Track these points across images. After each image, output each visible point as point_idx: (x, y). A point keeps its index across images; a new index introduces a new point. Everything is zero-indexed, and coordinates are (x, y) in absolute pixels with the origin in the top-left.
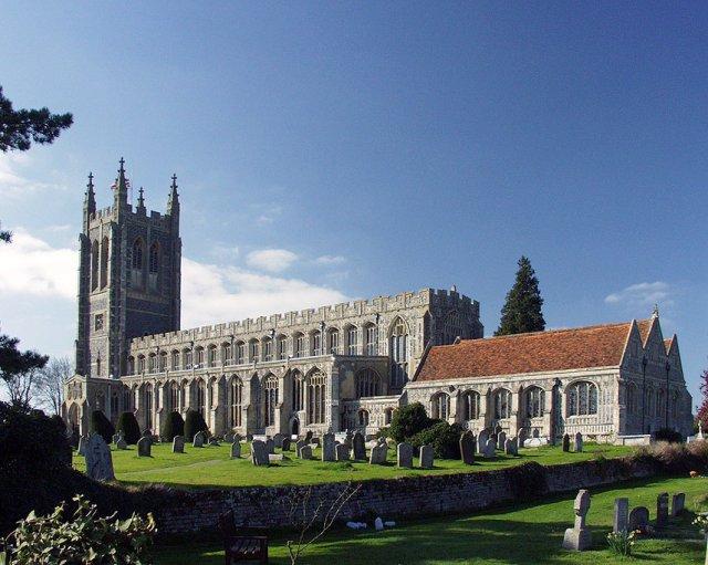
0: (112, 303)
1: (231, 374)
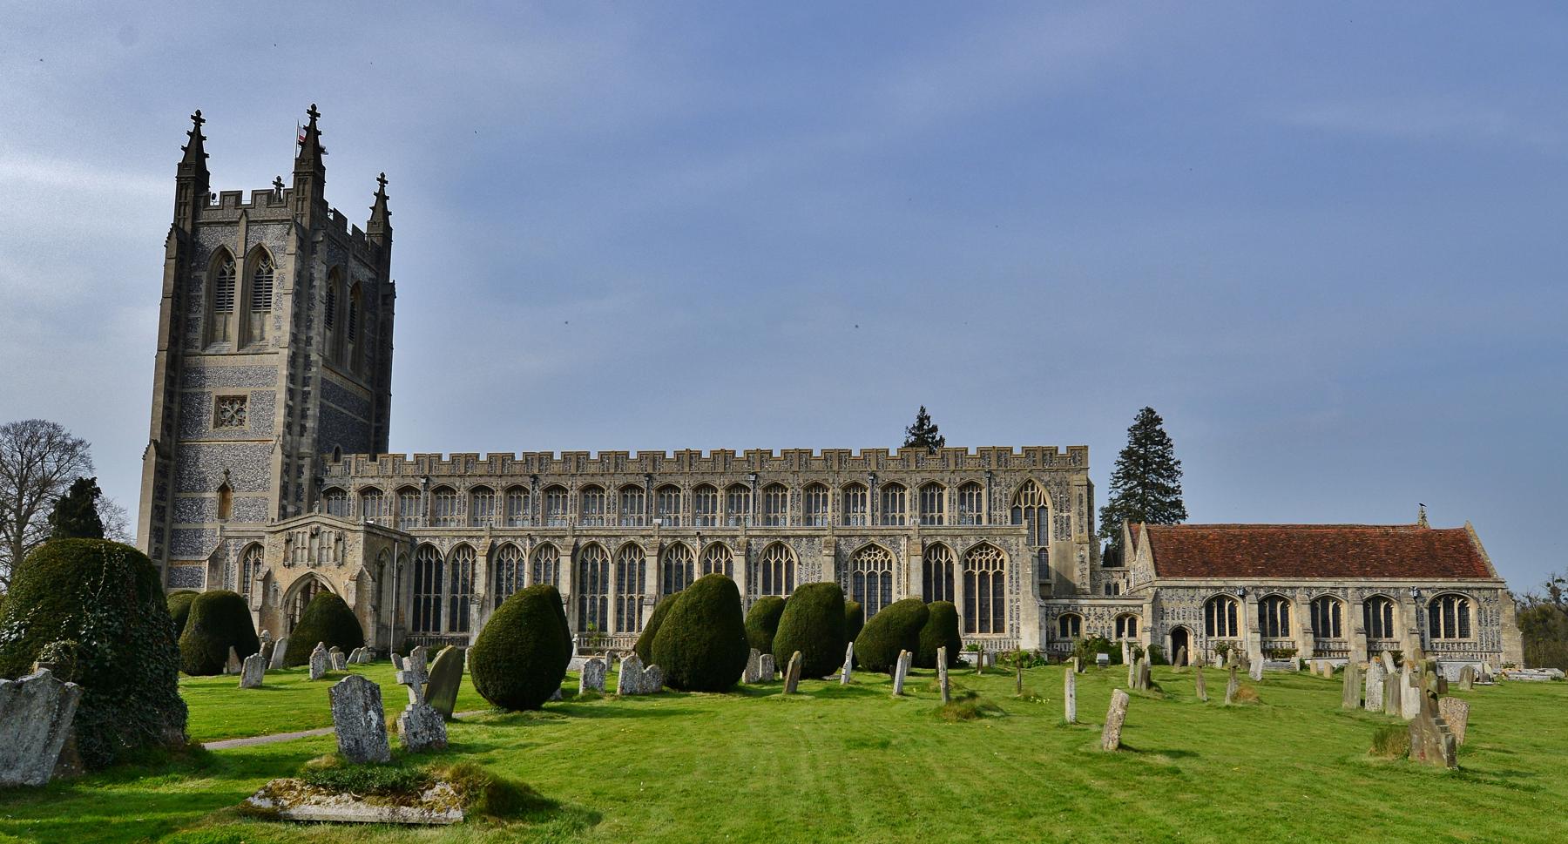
0: (292, 378)
1: (766, 542)
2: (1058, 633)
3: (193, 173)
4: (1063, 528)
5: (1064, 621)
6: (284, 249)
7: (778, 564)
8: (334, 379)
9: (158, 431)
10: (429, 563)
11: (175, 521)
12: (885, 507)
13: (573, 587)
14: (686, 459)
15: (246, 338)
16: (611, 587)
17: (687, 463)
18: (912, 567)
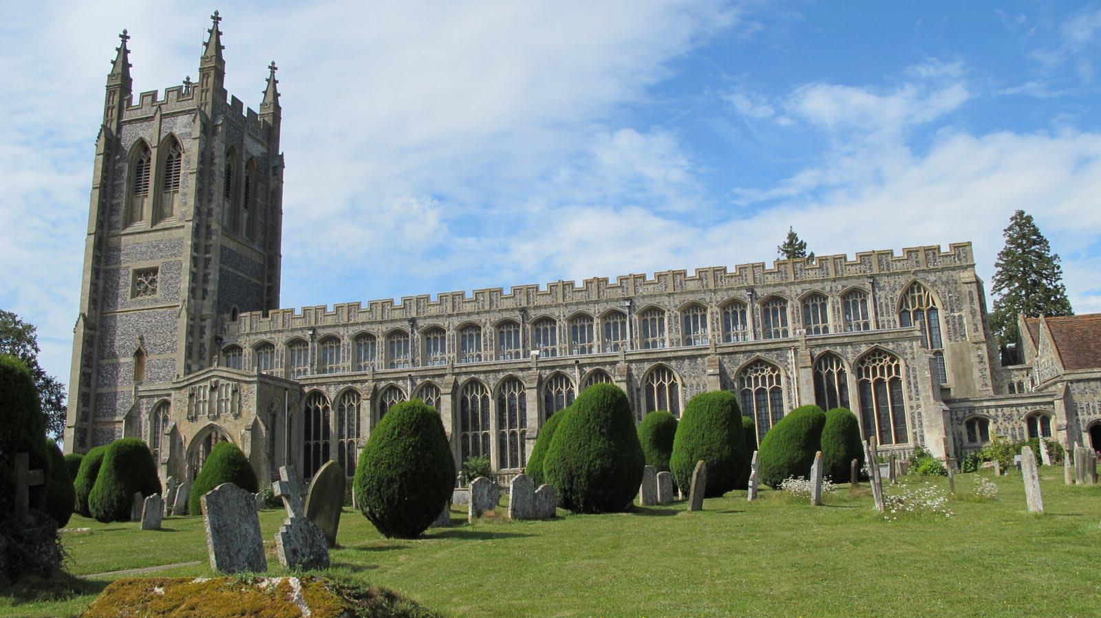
0: (195, 247)
1: (647, 366)
2: (965, 438)
3: (120, 82)
4: (956, 329)
5: (970, 425)
6: (190, 134)
7: (661, 387)
8: (232, 245)
9: (86, 306)
10: (317, 408)
11: (98, 386)
12: (766, 321)
13: (455, 426)
14: (560, 290)
15: (159, 214)
16: (493, 423)
17: (560, 295)
18: (802, 381)
